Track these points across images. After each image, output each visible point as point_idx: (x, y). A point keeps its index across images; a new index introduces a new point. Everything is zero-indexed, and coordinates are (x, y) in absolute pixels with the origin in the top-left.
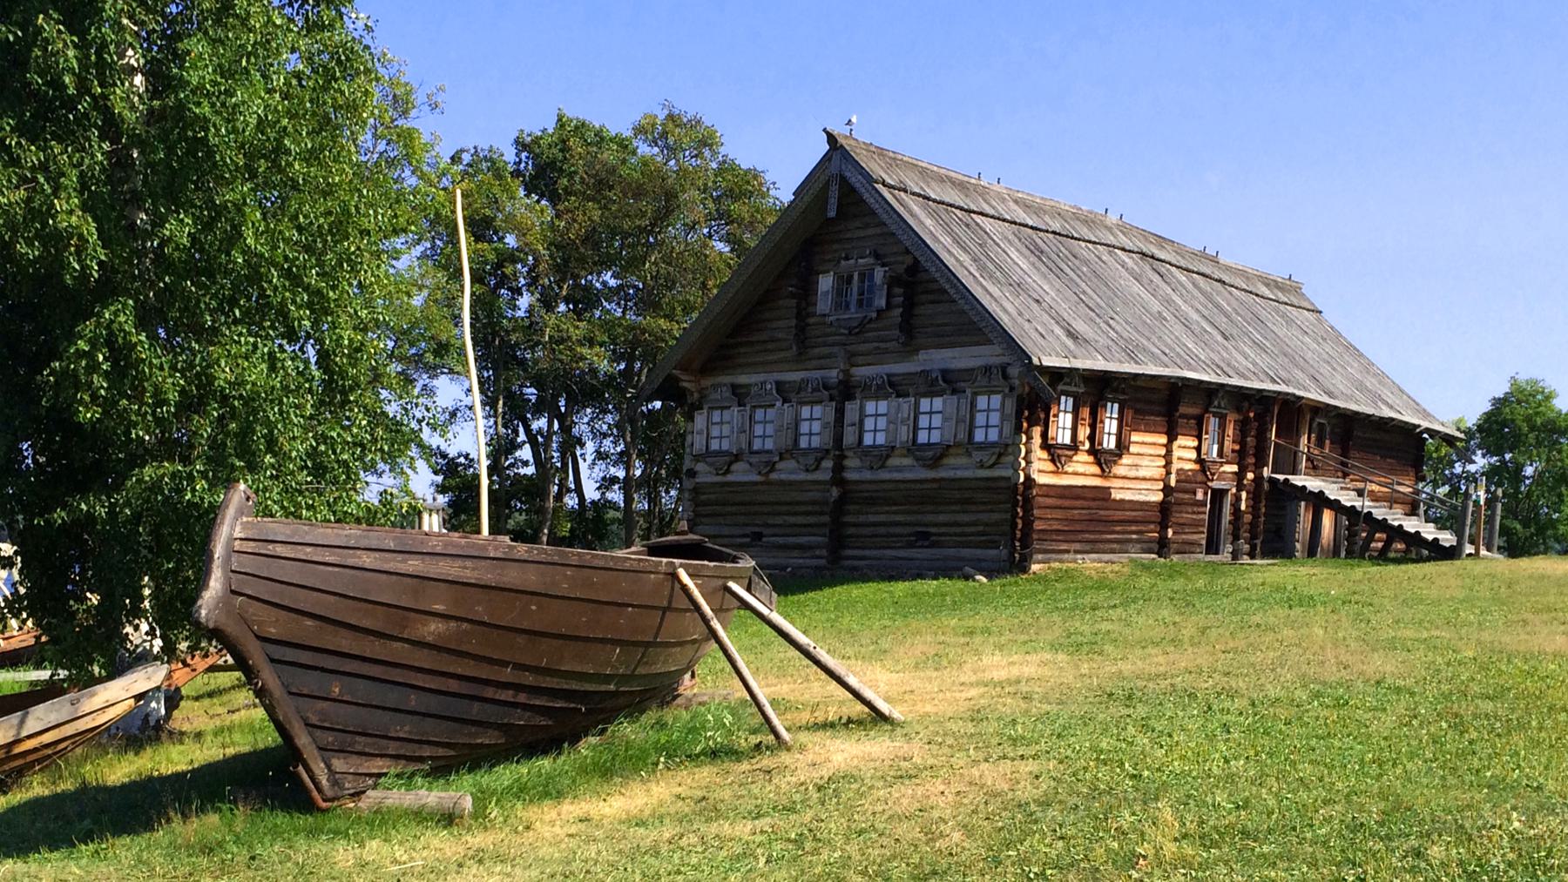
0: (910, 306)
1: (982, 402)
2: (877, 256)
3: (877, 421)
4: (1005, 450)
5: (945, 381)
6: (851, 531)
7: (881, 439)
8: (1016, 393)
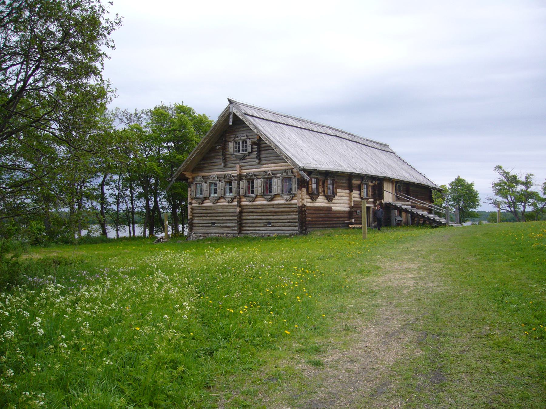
0: (259, 151)
2: (247, 136)
8: (296, 178)
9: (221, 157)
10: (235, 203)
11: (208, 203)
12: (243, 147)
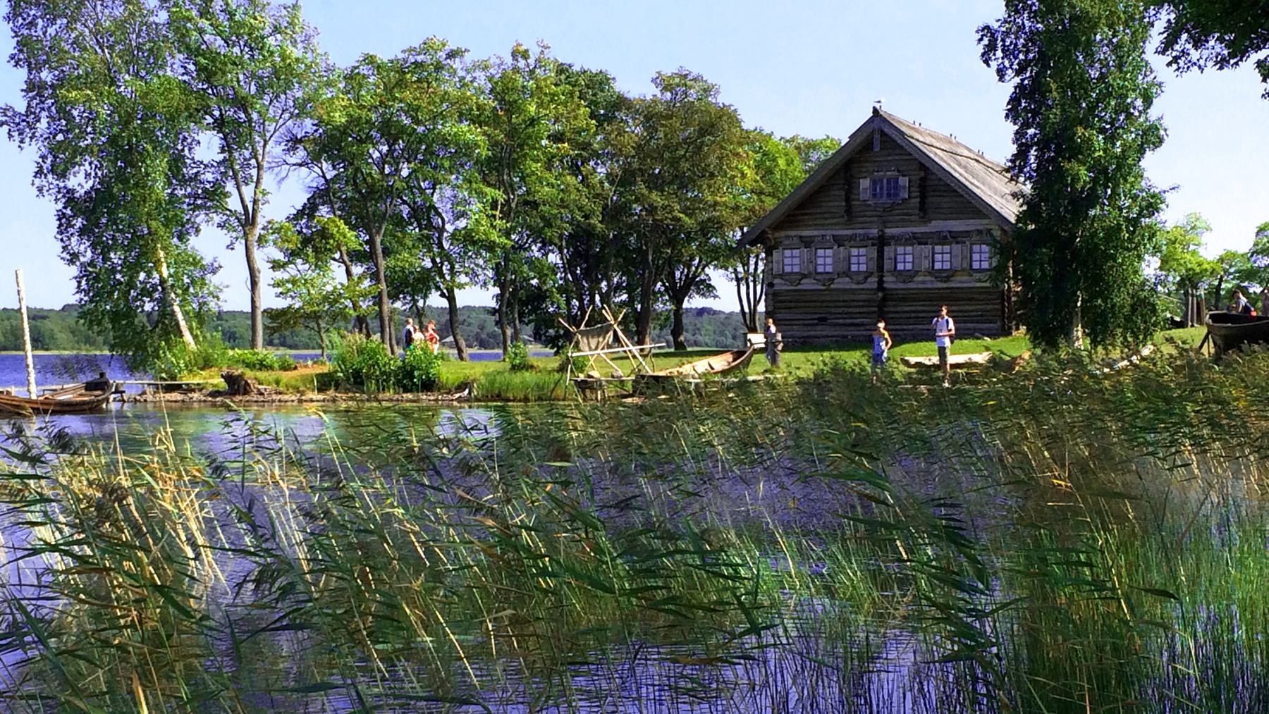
0: (923, 198)
3: (906, 258)
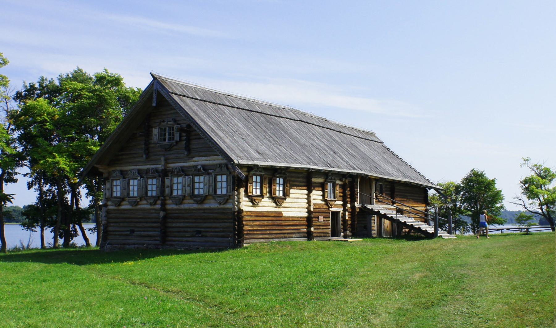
0: (189, 140)
1: (219, 178)
3: (178, 186)
4: (228, 198)
5: (204, 170)
6: (170, 230)
7: (180, 193)
9: (143, 146)
10: (158, 206)
11: (125, 206)
12: (170, 134)
